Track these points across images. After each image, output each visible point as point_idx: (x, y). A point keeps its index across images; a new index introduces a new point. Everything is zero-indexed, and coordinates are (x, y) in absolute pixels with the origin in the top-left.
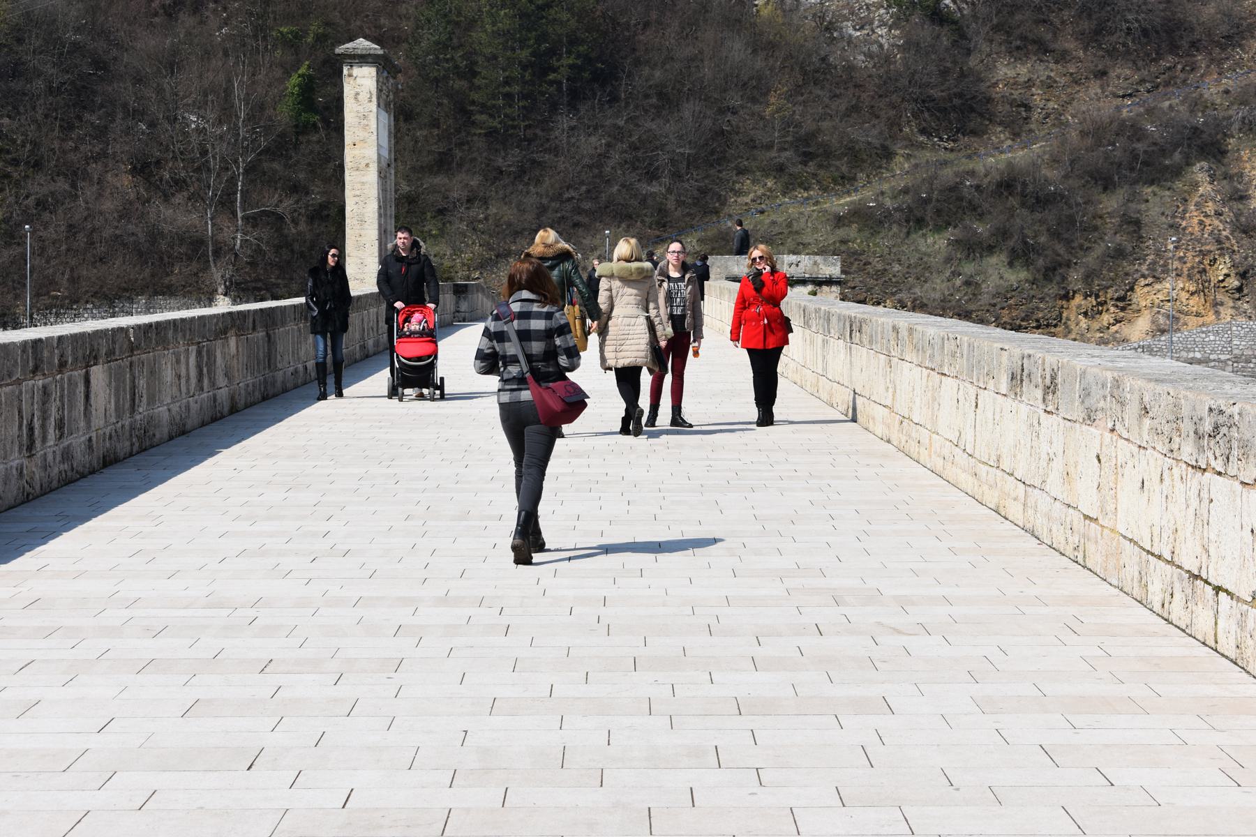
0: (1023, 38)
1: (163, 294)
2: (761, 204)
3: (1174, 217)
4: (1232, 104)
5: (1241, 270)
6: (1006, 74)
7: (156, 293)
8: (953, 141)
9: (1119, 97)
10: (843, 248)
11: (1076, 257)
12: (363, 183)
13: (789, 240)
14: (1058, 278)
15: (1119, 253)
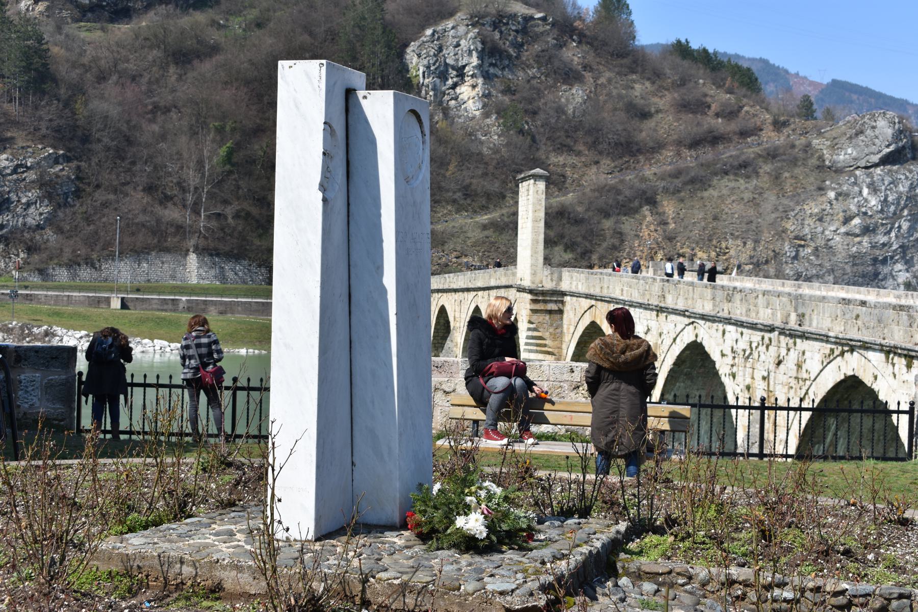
0: (561, 144)
1: (164, 251)
3: (636, 231)
4: (658, 179)
5: (668, 257)
7: (160, 251)
10: (487, 240)
14: (586, 258)
15: (614, 248)
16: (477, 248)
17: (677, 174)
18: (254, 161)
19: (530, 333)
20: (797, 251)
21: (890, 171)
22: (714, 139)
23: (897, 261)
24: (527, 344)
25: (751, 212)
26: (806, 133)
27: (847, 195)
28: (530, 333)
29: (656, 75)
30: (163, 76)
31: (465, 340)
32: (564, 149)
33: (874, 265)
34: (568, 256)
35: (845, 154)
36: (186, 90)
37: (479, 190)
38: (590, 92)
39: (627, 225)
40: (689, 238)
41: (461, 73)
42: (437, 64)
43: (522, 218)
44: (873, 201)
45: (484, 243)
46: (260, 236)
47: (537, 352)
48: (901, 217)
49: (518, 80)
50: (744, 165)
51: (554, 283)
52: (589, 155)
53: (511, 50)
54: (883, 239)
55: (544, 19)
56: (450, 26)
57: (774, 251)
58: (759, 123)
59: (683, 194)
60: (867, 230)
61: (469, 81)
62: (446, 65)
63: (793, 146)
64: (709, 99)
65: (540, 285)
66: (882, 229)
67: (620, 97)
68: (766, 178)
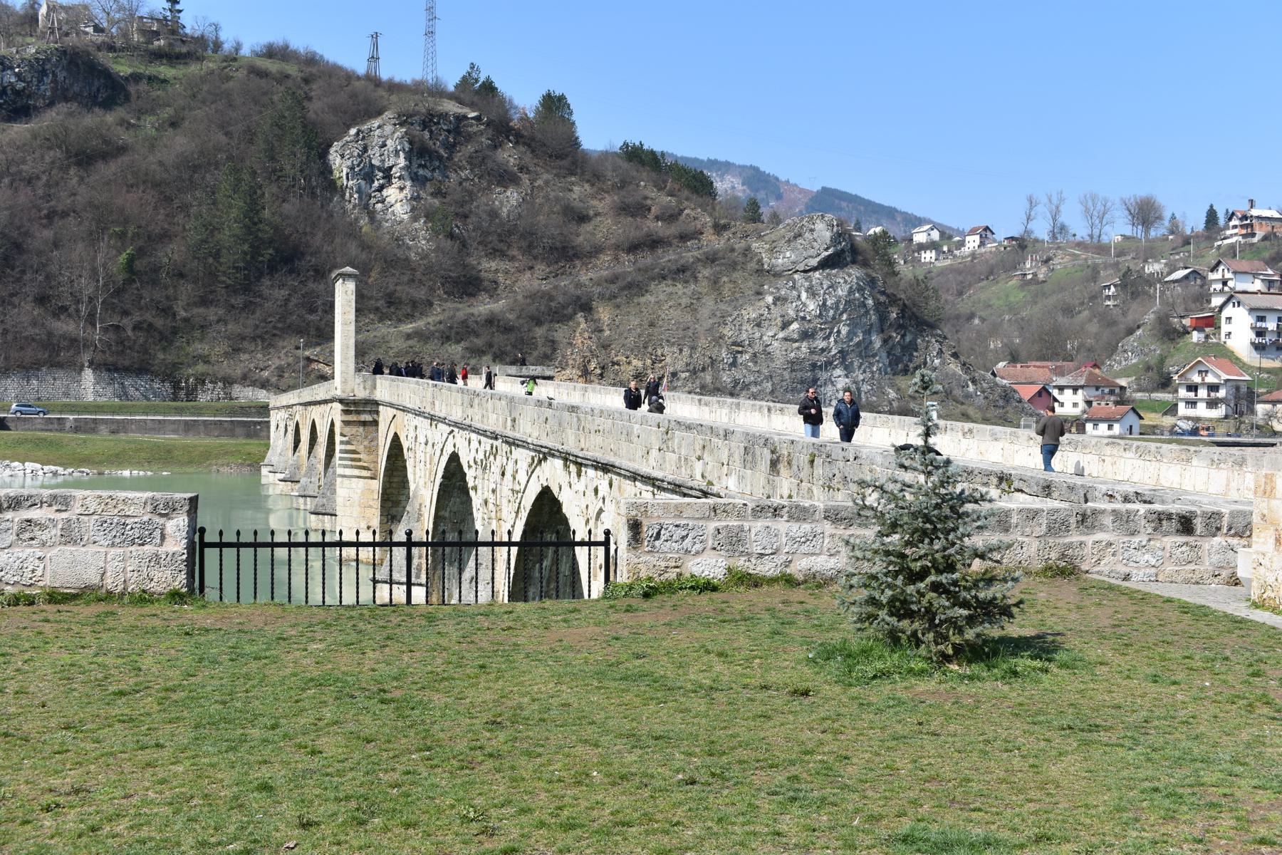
0: (494, 249)
7: (52, 366)
17: (613, 280)
18: (160, 268)
20: (735, 358)
21: (828, 274)
22: (654, 243)
23: (836, 366)
24: (341, 459)
25: (688, 318)
26: (747, 236)
27: (785, 299)
28: (344, 447)
29: (595, 177)
30: (62, 178)
32: (498, 254)
33: (813, 371)
35: (784, 258)
36: (83, 195)
37: (404, 297)
38: (526, 194)
39: (561, 333)
44: (812, 306)
45: (407, 353)
46: (164, 349)
47: (352, 467)
48: (840, 321)
50: (683, 270)
51: (368, 391)
52: (522, 260)
53: (442, 152)
54: (822, 344)
55: (478, 119)
56: (376, 125)
57: (711, 358)
58: (699, 226)
60: (806, 335)
62: (372, 166)
63: (733, 250)
64: (649, 202)
66: (821, 334)
67: (557, 199)
68: (705, 283)
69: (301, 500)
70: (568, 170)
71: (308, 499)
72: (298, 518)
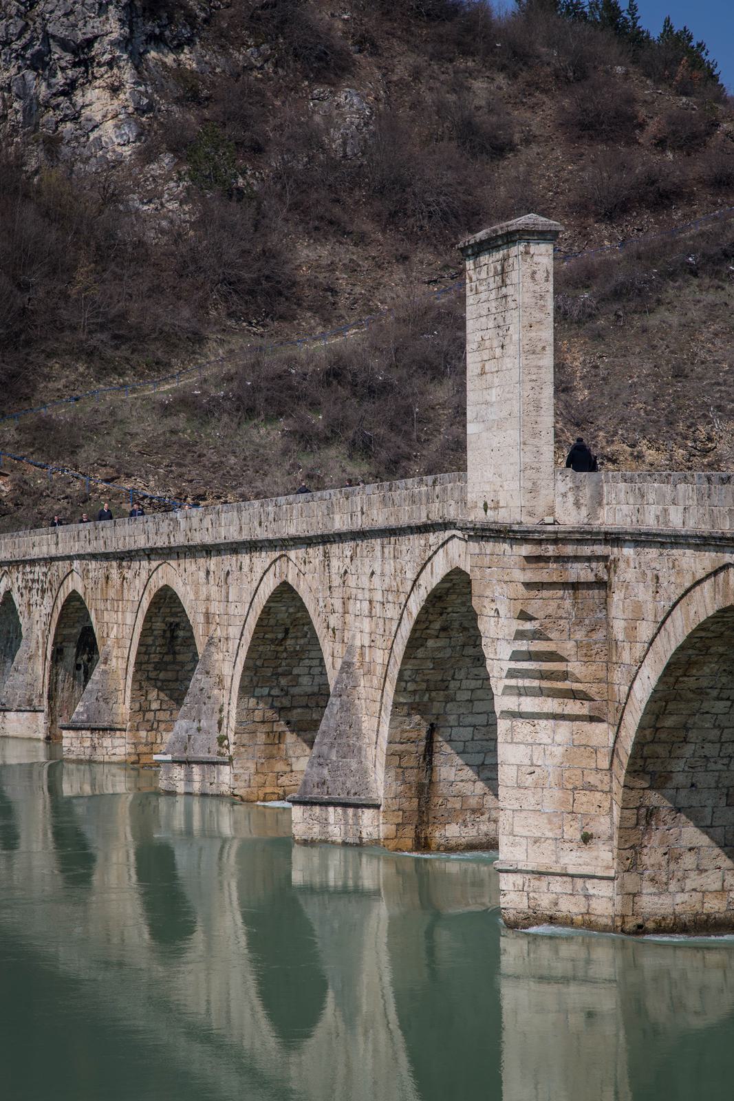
0: (322, 218)
2: (74, 390)
6: (308, 256)
8: (263, 326)
9: (425, 282)
10: (174, 438)
11: (415, 450)
12: (540, 368)
13: (115, 430)
16: (154, 458)
19: (523, 646)
24: (512, 674)
28: (523, 646)
31: (246, 668)
34: (358, 469)
40: (623, 420)
41: (82, 54)
42: (27, 36)
43: (480, 347)
45: (167, 445)
47: (541, 692)
49: (213, 72)
51: (584, 511)
59: (601, 322)
61: (105, 76)
62: (47, 36)
65: (549, 520)
67: (441, 108)
69: (179, 772)
70: (459, 44)
71: (196, 769)
72: (170, 817)
